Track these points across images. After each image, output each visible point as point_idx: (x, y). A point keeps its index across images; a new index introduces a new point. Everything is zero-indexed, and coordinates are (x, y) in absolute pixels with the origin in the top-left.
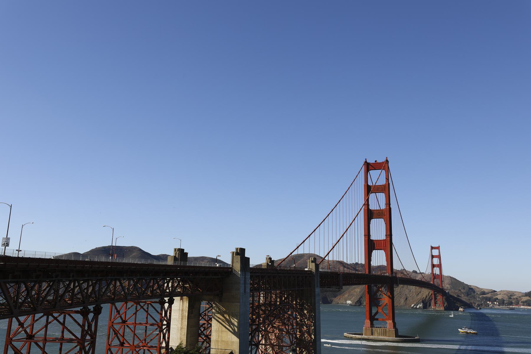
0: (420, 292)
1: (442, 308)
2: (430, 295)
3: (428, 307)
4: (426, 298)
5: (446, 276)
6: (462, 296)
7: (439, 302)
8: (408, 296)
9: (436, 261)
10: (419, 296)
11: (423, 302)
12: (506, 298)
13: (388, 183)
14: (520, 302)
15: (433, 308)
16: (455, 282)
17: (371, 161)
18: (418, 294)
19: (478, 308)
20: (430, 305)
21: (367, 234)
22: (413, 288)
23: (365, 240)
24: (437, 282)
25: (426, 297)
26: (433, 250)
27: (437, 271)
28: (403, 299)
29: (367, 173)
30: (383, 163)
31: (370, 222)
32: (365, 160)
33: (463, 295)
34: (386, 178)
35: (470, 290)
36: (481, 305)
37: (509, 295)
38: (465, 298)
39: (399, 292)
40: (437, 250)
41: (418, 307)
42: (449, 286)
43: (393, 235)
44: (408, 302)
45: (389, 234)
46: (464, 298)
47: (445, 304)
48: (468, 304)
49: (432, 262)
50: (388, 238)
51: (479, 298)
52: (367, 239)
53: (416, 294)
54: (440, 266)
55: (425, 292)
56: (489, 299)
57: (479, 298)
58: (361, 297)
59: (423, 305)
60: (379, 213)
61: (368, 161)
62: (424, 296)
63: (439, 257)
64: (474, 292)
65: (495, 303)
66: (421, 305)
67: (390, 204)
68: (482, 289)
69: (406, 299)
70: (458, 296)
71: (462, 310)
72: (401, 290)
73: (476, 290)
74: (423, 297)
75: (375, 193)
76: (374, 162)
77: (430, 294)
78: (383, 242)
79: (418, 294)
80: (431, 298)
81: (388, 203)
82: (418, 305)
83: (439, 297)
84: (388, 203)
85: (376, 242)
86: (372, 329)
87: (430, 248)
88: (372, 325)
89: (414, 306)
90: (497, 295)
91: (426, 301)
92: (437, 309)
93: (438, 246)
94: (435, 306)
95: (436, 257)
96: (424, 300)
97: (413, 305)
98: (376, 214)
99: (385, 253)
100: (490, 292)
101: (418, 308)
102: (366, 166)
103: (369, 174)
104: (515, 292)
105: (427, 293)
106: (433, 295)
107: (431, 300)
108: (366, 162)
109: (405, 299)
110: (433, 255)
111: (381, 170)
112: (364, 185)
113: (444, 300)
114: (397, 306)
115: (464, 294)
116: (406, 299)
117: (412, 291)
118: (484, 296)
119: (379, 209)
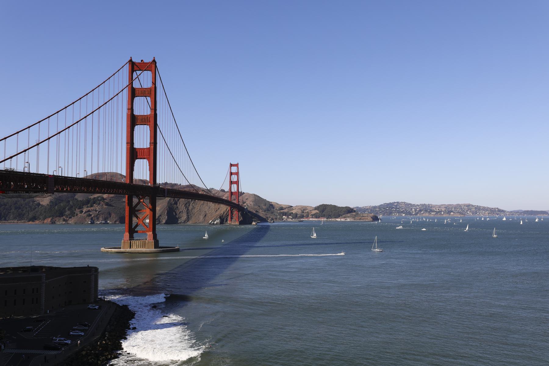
0: (219, 209)
1: (237, 223)
3: (224, 222)
5: (251, 194)
6: (260, 211)
7: (235, 218)
8: (207, 212)
9: (234, 178)
10: (218, 213)
11: (220, 218)
12: (299, 212)
14: (310, 215)
15: (229, 223)
16: (258, 199)
19: (272, 222)
20: (227, 221)
22: (211, 204)
25: (224, 213)
28: (202, 215)
33: (261, 211)
34: (152, 82)
35: (270, 206)
36: (276, 219)
37: (302, 210)
38: (263, 213)
39: (198, 209)
41: (215, 223)
42: (252, 203)
44: (207, 218)
46: (262, 214)
47: (240, 218)
48: (264, 218)
49: (230, 179)
50: (152, 146)
51: (277, 213)
54: (237, 183)
55: (223, 209)
56: (285, 214)
57: (277, 213)
58: (160, 215)
59: (220, 220)
62: (222, 212)
63: (237, 174)
64: (274, 208)
65: (290, 217)
66: (218, 221)
68: (281, 205)
69: (206, 215)
70: (257, 211)
71: (255, 224)
73: (277, 206)
77: (228, 210)
78: (147, 151)
80: (228, 214)
82: (215, 221)
83: (235, 213)
89: (212, 222)
90: (293, 209)
92: (232, 224)
94: (231, 221)
96: (221, 215)
97: (211, 221)
98: (140, 120)
100: (287, 208)
101: (216, 224)
104: (308, 206)
105: (225, 209)
106: (230, 211)
107: (228, 215)
109: (204, 216)
110: (232, 172)
113: (240, 215)
114: (196, 223)
115: (262, 210)
116: (206, 215)
117: (211, 208)
118: (282, 211)
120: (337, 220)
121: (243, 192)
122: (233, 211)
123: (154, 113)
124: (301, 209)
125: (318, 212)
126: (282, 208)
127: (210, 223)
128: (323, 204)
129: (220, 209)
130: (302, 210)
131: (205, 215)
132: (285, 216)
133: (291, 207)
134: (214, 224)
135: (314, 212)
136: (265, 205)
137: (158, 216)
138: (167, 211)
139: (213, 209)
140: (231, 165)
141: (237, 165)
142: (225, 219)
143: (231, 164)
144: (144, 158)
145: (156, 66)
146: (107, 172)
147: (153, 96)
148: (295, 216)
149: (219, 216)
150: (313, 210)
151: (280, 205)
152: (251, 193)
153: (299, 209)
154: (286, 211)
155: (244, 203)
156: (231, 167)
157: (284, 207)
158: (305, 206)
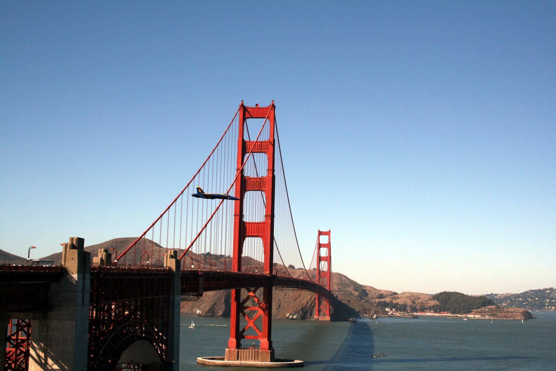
1: (328, 318)
2: (312, 301)
4: (306, 305)
9: (324, 252)
13: (273, 139)
16: (345, 282)
18: (296, 299)
20: (311, 315)
21: (238, 213)
24: (324, 282)
25: (308, 303)
26: (321, 236)
27: (324, 266)
28: (275, 306)
29: (243, 123)
30: (267, 108)
31: (244, 195)
32: (240, 103)
40: (327, 237)
45: (271, 215)
49: (319, 253)
52: (238, 220)
53: (293, 298)
54: (328, 259)
55: (307, 296)
60: (257, 183)
61: (245, 105)
62: (305, 302)
63: (328, 246)
67: (273, 170)
74: (303, 303)
76: (254, 106)
77: (313, 299)
79: (296, 299)
81: (272, 170)
84: (272, 170)
86: (238, 352)
87: (317, 233)
88: (238, 346)
89: (290, 315)
91: (307, 309)
93: (328, 230)
96: (304, 307)
97: (288, 315)
98: (253, 184)
102: (242, 111)
103: (245, 123)
105: (309, 297)
106: (317, 300)
108: (242, 105)
110: (321, 242)
111: (265, 119)
112: (238, 140)
116: (280, 306)
119: (256, 176)
120: (468, 316)
122: (321, 301)
124: (411, 297)
125: (437, 303)
126: (381, 296)
127: (288, 318)
128: (445, 292)
129: (301, 297)
130: (412, 300)
131: (278, 305)
132: (387, 307)
133: (396, 293)
134: (292, 319)
135: (433, 303)
136: (356, 291)
137: (212, 305)
138: (224, 297)
140: (320, 233)
142: (309, 311)
144: (258, 236)
146: (172, 248)
148: (402, 308)
149: (300, 308)
150: (429, 300)
151: (379, 290)
153: (408, 297)
154: (388, 300)
156: (320, 236)
157: (384, 293)
158: (416, 293)
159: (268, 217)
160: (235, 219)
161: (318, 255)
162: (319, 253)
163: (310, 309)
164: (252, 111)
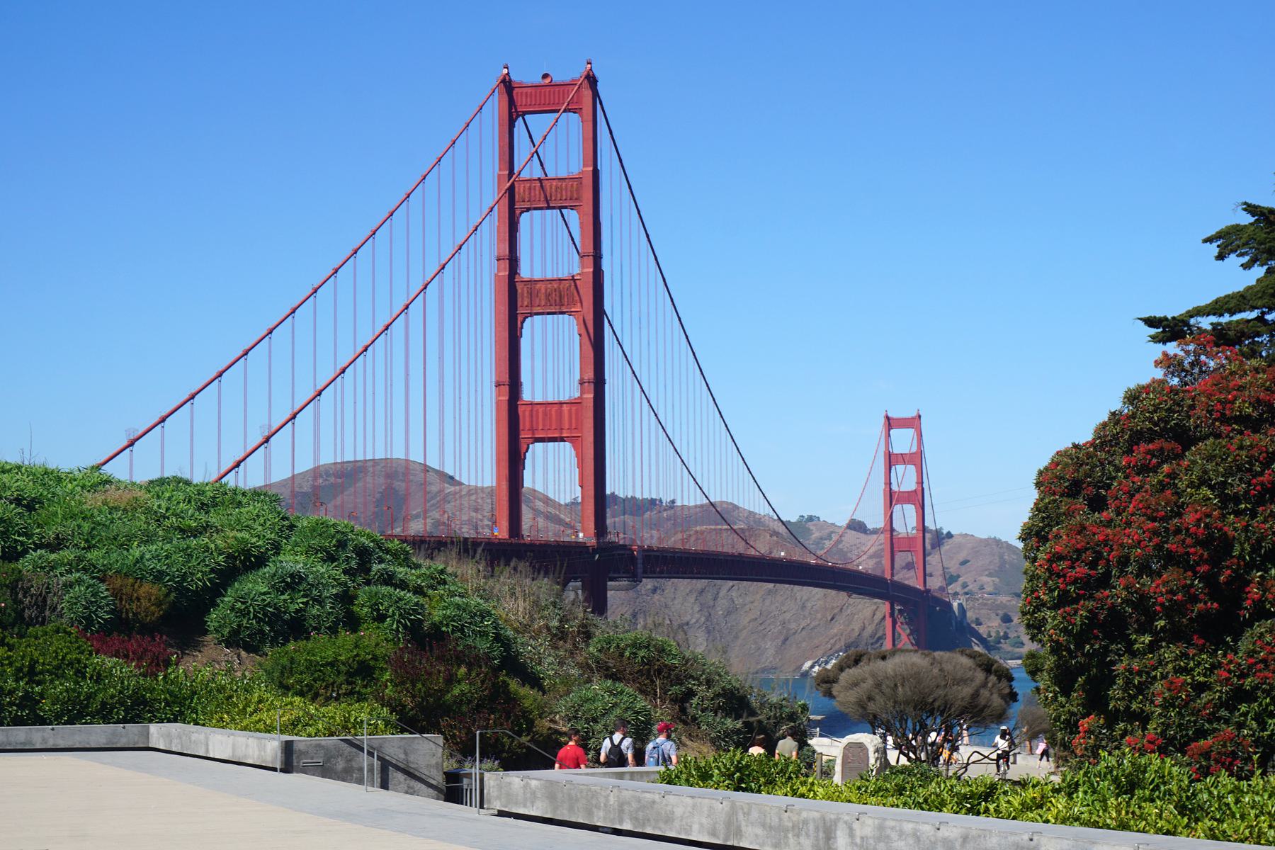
2: (876, 622)
17: (526, 75)
23: (498, 403)
40: (911, 431)
43: (607, 381)
49: (889, 483)
50: (588, 392)
54: (917, 498)
62: (856, 627)
63: (916, 459)
72: (767, 602)
75: (560, 208)
77: (879, 616)
85: (541, 410)
87: (882, 420)
89: (812, 667)
95: (904, 459)
99: (573, 453)
105: (867, 612)
109: (779, 642)
111: (556, 115)
117: (809, 605)
121: (945, 532)
123: (591, 270)
131: (782, 638)
139: (817, 612)
140: (890, 423)
141: (913, 423)
143: (888, 418)
144: (562, 439)
145: (596, 95)
147: (588, 208)
152: (982, 534)
155: (952, 579)
159: (586, 384)
160: (499, 394)
161: (885, 487)
162: (889, 483)
163: (872, 644)
164: (533, 93)
